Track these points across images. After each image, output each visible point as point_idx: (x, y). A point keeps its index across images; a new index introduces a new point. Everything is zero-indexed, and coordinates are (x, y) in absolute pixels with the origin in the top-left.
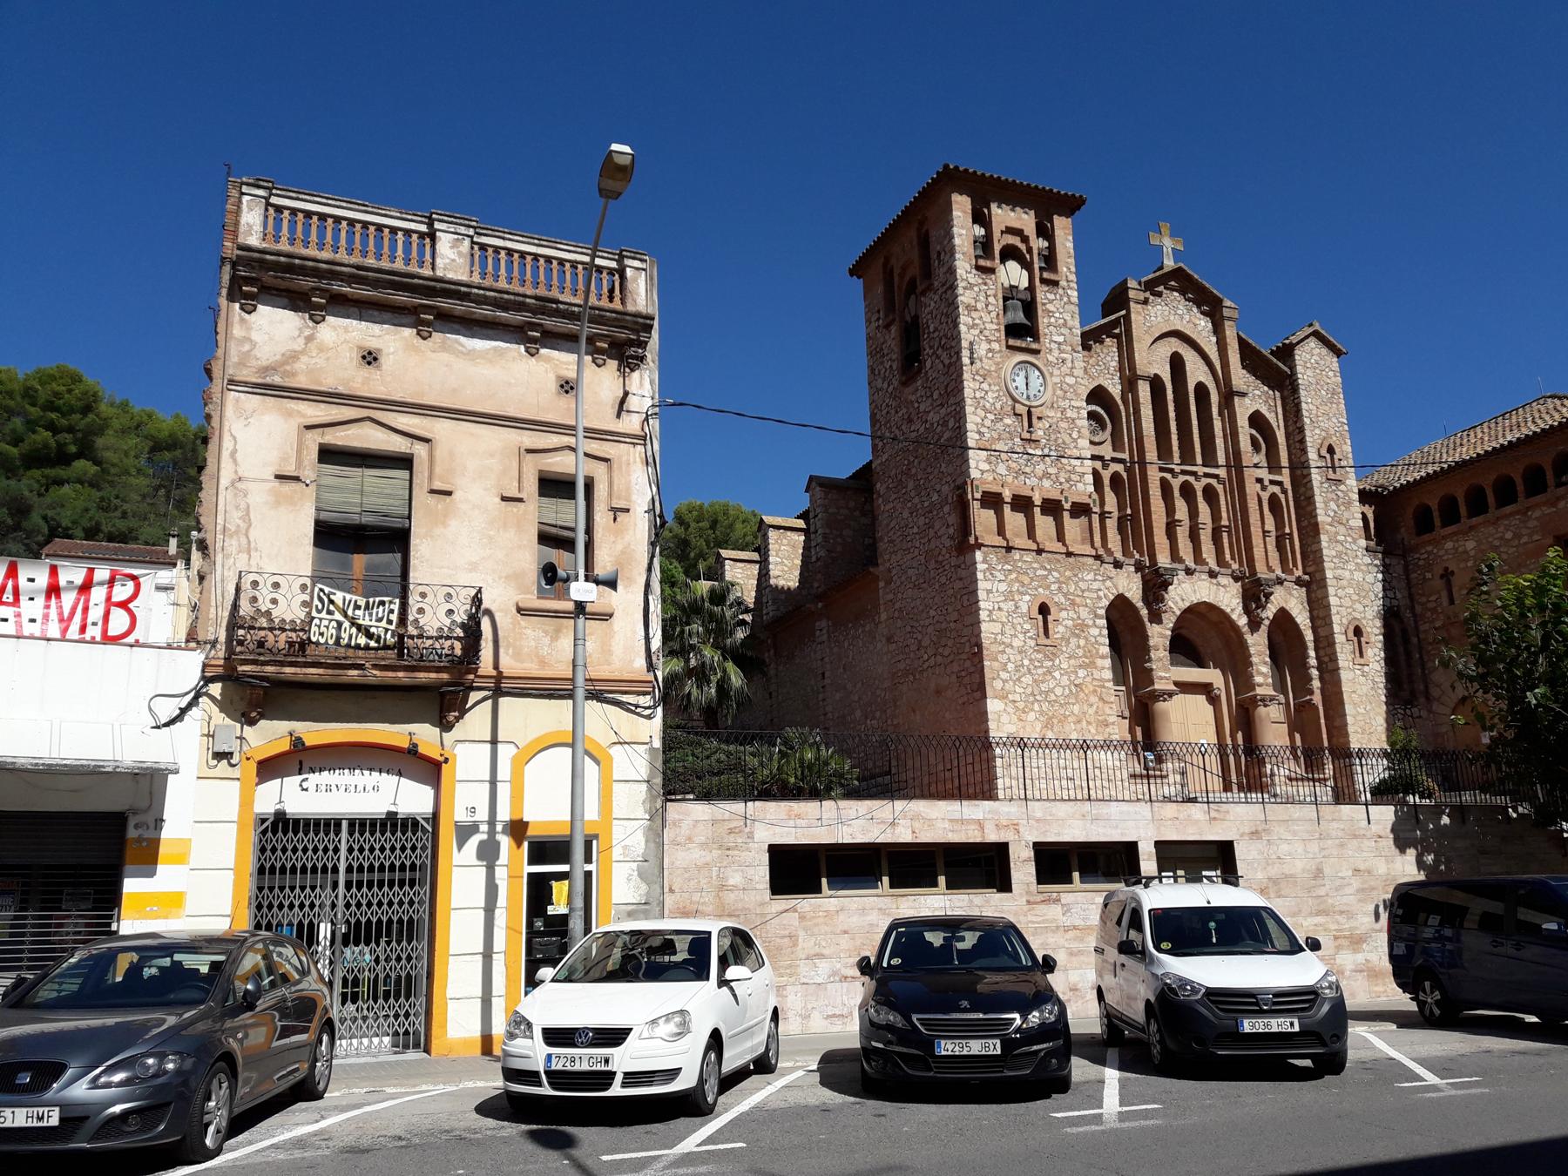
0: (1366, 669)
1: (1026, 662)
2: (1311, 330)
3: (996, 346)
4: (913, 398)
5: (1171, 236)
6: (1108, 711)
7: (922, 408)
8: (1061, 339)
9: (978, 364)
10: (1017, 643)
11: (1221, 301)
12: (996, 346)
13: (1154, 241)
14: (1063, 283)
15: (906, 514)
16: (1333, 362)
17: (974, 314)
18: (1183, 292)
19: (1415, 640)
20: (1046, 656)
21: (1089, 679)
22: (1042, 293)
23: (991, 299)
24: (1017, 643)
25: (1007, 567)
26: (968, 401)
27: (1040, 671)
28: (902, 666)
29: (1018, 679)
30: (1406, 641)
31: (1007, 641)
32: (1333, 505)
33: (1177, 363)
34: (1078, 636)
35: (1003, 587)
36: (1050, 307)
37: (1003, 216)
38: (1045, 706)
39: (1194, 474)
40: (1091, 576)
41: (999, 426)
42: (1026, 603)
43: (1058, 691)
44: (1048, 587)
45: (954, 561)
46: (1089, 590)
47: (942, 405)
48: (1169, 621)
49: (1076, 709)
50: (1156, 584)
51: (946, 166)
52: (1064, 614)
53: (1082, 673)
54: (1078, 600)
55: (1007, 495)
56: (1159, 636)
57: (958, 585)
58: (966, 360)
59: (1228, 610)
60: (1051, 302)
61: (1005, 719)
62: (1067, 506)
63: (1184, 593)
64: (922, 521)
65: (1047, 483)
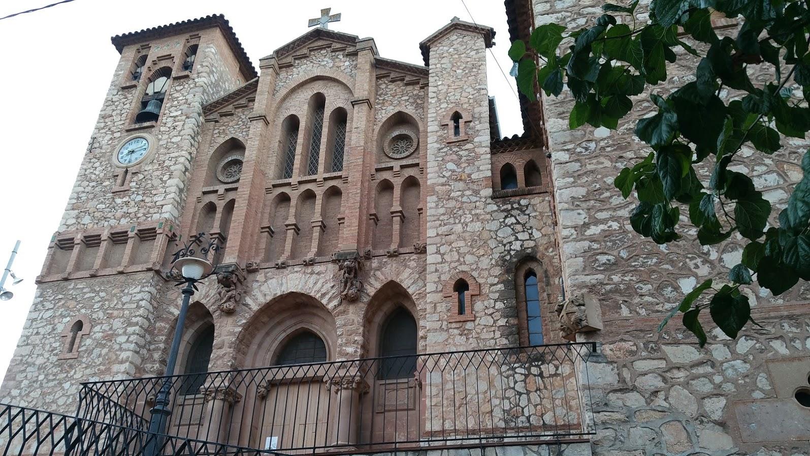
0: (469, 325)
1: (41, 377)
3: (117, 135)
24: (40, 361)
32: (451, 166)
33: (319, 102)
42: (64, 325)
46: (131, 302)
65: (124, 221)
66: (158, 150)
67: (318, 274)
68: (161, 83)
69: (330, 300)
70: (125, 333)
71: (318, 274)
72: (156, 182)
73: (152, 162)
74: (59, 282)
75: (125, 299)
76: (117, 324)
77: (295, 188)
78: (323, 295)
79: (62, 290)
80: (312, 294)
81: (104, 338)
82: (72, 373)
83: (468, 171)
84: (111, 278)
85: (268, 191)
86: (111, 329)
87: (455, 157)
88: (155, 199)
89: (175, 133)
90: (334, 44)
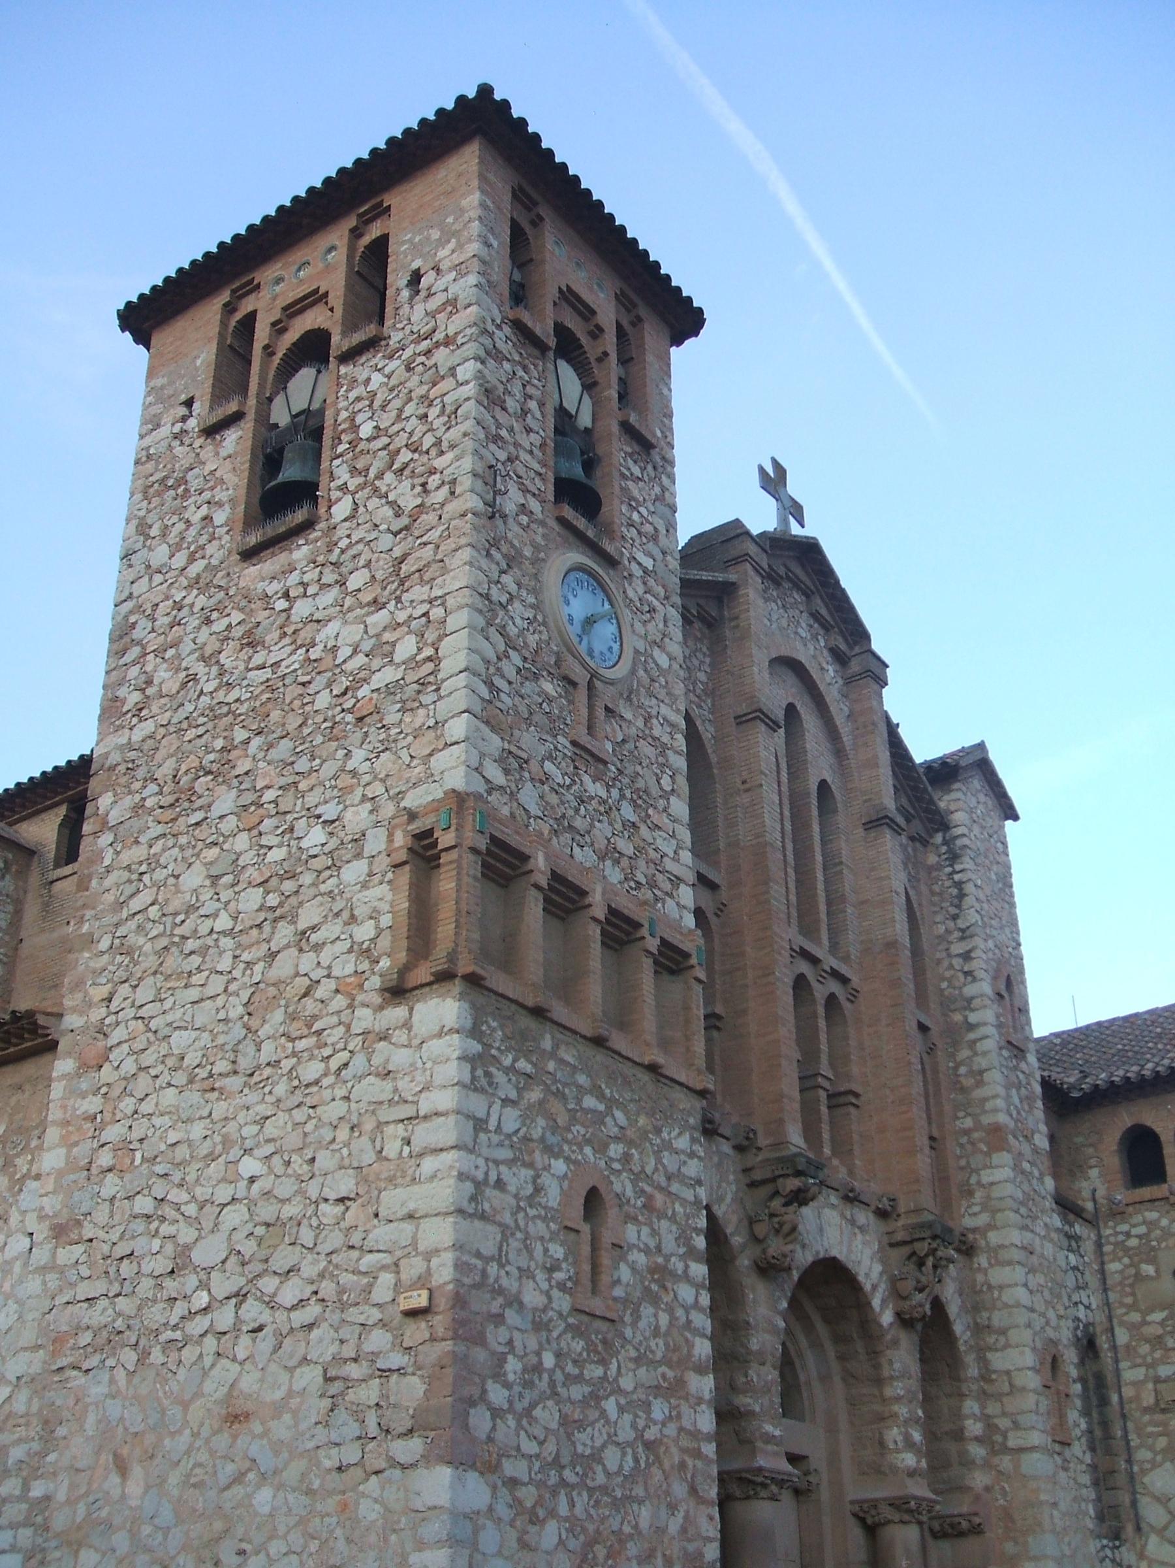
0: (1067, 1453)
1: (549, 1360)
3: (534, 505)
4: (274, 587)
7: (302, 609)
8: (648, 563)
10: (532, 1298)
12: (534, 505)
15: (194, 878)
17: (498, 412)
19: (1115, 1398)
20: (591, 1348)
21: (671, 1430)
22: (618, 453)
23: (533, 405)
25: (523, 1065)
27: (577, 1392)
28: (98, 1315)
29: (528, 1412)
30: (1104, 1402)
31: (510, 1284)
34: (655, 1300)
35: (511, 1120)
38: (582, 1500)
39: (814, 961)
41: (529, 687)
43: (612, 1458)
44: (601, 1148)
45: (364, 1018)
47: (377, 604)
49: (645, 1514)
51: (485, 91)
52: (631, 1233)
53: (659, 1410)
54: (659, 1199)
55: (540, 861)
57: (373, 1089)
59: (868, 1287)
61: (489, 1538)
62: (653, 944)
64: (252, 899)
65: (614, 875)
70: (686, 1277)
74: (514, 1007)
79: (521, 1043)
80: (861, 1278)
82: (614, 1366)
84: (628, 1070)
90: (819, 601)
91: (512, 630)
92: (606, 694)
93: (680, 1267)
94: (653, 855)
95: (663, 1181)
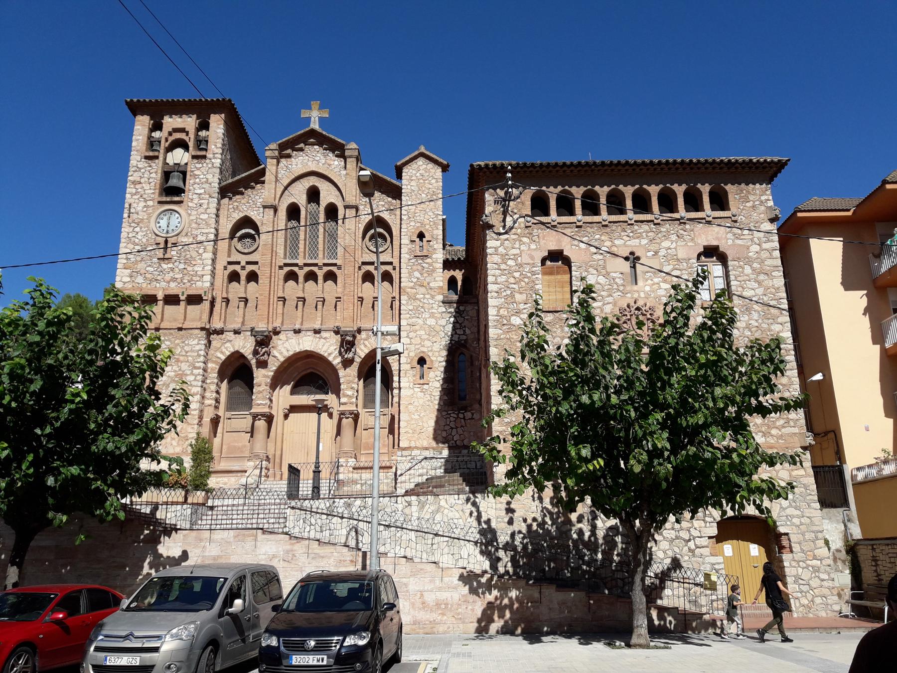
0: (425, 387)
2: (416, 153)
3: (150, 203)
5: (321, 108)
6: (190, 430)
8: (202, 191)
9: (134, 216)
11: (343, 145)
12: (150, 203)
13: (304, 114)
14: (209, 155)
16: (438, 172)
17: (138, 186)
18: (320, 145)
26: (123, 240)
32: (417, 274)
33: (313, 195)
36: (197, 172)
37: (170, 122)
40: (196, 342)
46: (192, 351)
48: (273, 366)
50: (263, 341)
54: (182, 358)
56: (262, 377)
58: (126, 215)
59: (326, 355)
60: (198, 169)
63: (285, 347)
65: (173, 285)
66: (190, 225)
67: (325, 338)
68: (178, 156)
69: (335, 358)
70: (192, 374)
71: (325, 338)
72: (194, 254)
73: (187, 235)
75: (187, 348)
76: (184, 366)
77: (301, 268)
78: (330, 354)
81: (176, 376)
83: (428, 279)
85: (281, 268)
86: (180, 370)
87: (420, 268)
88: (196, 268)
89: (201, 210)
91: (137, 241)
92: (171, 241)
93: (189, 372)
94: (192, 273)
95: (184, 353)
